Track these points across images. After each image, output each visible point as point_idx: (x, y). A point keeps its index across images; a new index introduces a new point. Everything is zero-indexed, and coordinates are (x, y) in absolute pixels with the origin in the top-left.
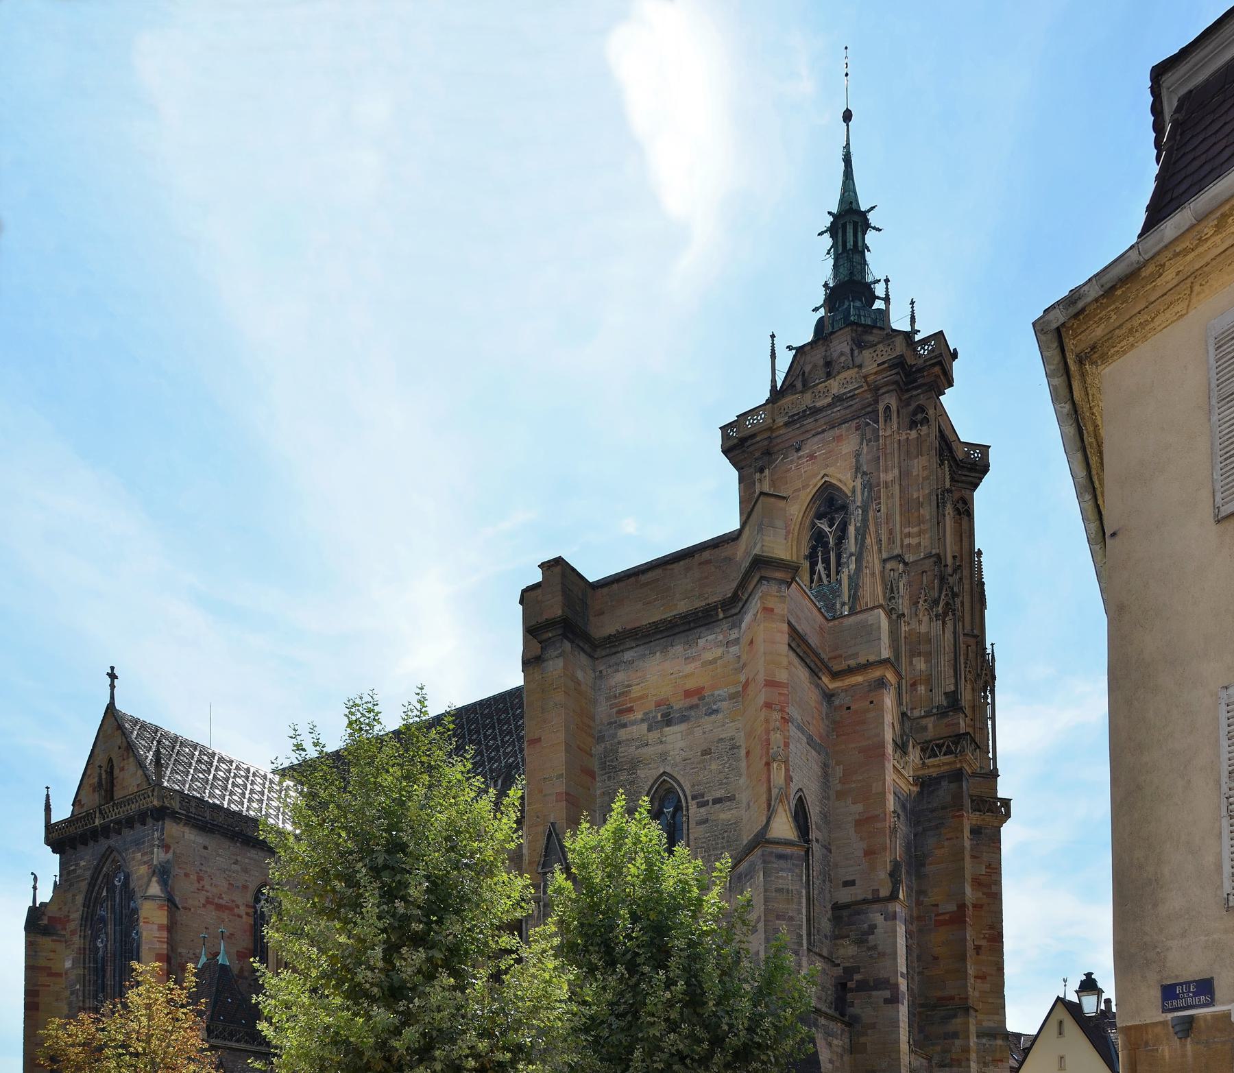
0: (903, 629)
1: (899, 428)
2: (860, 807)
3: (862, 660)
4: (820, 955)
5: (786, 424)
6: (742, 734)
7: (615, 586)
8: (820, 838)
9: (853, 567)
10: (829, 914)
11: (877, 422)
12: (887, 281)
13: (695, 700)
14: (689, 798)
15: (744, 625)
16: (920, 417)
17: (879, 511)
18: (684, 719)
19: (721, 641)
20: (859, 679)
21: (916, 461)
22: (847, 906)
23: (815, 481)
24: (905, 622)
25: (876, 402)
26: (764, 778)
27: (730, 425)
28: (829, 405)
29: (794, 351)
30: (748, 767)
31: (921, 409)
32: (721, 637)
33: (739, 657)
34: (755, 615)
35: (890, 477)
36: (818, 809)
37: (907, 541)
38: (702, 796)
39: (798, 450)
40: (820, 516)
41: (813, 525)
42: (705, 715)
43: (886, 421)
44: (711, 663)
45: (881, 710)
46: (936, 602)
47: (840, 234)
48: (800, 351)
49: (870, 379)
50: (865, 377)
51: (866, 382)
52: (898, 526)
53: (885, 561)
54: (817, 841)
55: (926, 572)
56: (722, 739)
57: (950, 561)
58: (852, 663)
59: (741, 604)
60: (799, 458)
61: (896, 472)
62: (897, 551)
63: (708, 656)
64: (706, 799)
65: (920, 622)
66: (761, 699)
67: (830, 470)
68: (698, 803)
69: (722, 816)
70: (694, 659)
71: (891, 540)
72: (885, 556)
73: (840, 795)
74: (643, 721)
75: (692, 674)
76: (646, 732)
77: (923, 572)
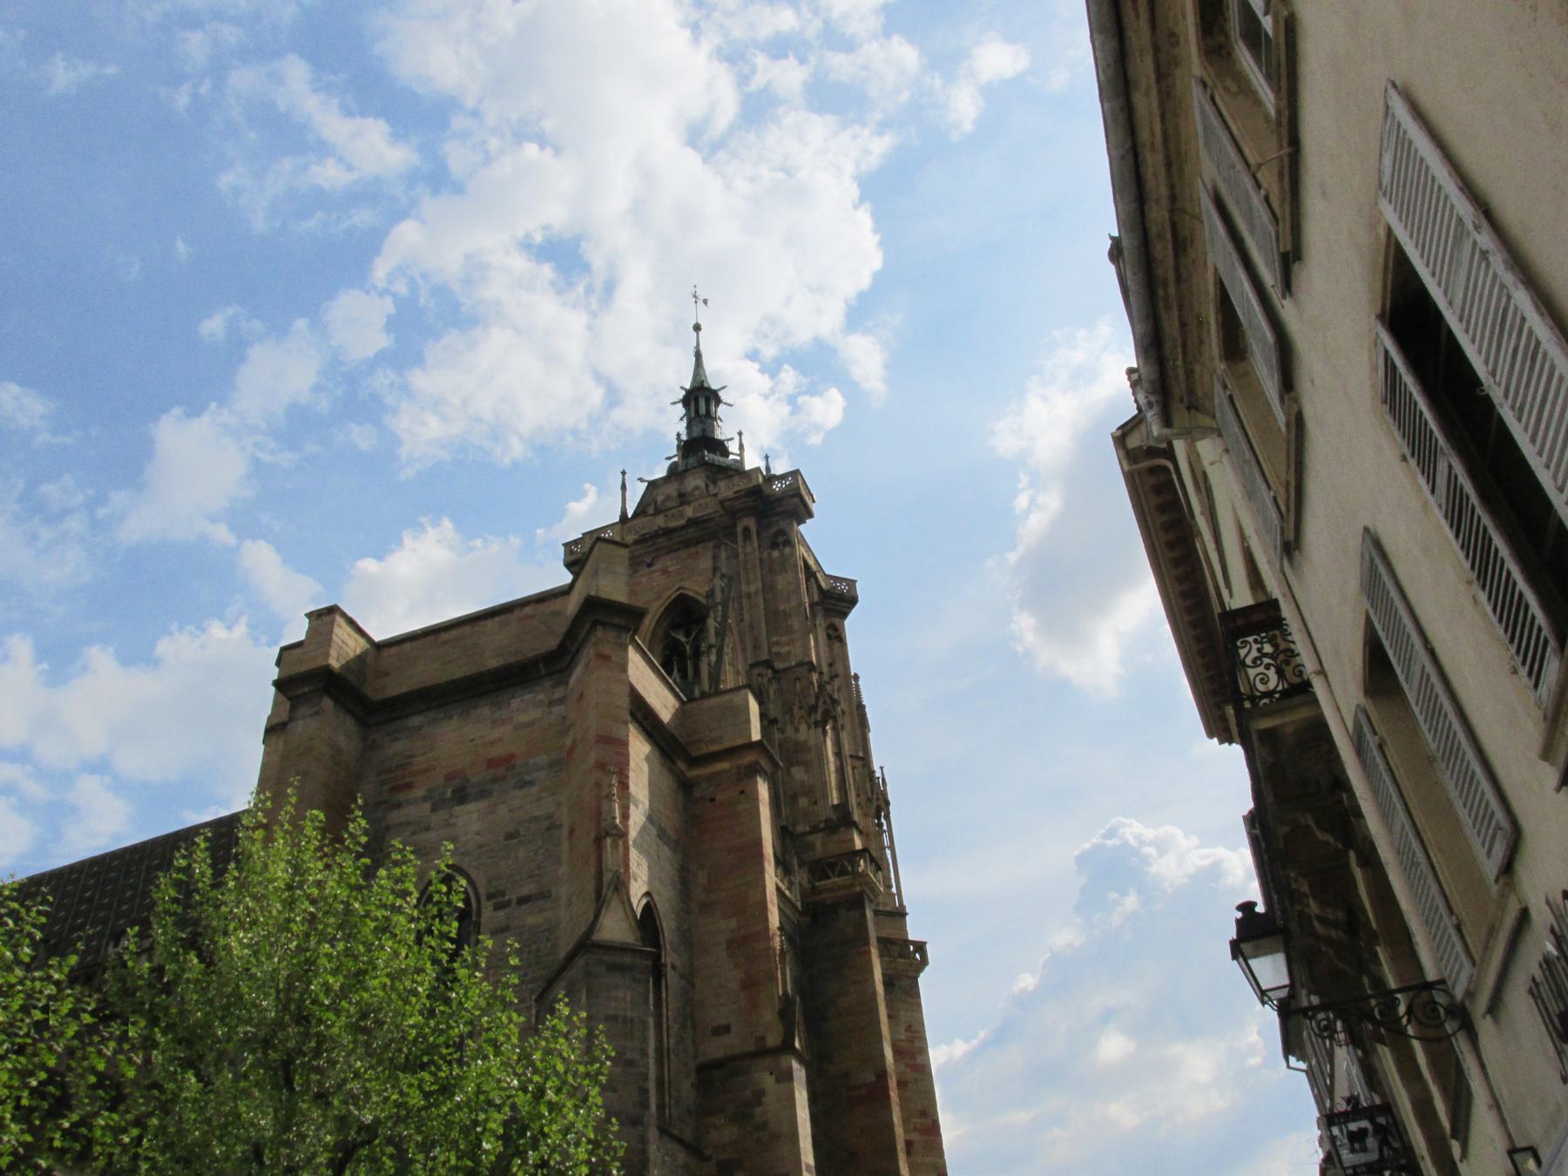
0: (776, 735)
1: (759, 547)
2: (733, 923)
3: (727, 744)
4: (680, 1141)
5: (637, 542)
6: (565, 810)
7: (407, 646)
8: (678, 964)
9: (713, 658)
10: (693, 1077)
11: (736, 543)
12: (740, 434)
13: (501, 771)
14: (483, 898)
15: (572, 681)
16: (781, 539)
17: (742, 621)
18: (483, 794)
19: (540, 701)
20: (723, 766)
21: (780, 578)
22: (718, 1065)
23: (669, 593)
24: (778, 729)
25: (735, 526)
26: (593, 861)
27: (575, 542)
28: (683, 527)
29: (646, 484)
30: (571, 849)
31: (783, 533)
32: (541, 697)
33: (564, 718)
34: (587, 666)
35: (753, 589)
36: (673, 924)
37: (775, 649)
38: (502, 894)
39: (650, 565)
40: (675, 627)
41: (667, 635)
42: (515, 788)
43: (745, 540)
44: (527, 725)
45: (755, 799)
46: (813, 709)
47: (693, 404)
48: (652, 485)
49: (727, 504)
50: (722, 502)
51: (723, 507)
52: (764, 635)
53: (753, 666)
54: (674, 967)
55: (799, 679)
56: (535, 818)
57: (825, 669)
58: (715, 748)
59: (569, 658)
60: (651, 572)
61: (759, 584)
62: (765, 657)
63: (523, 718)
64: (507, 898)
65: (797, 730)
66: (592, 758)
67: (686, 584)
68: (495, 904)
69: (531, 920)
70: (503, 722)
71: (756, 647)
72: (750, 662)
73: (706, 908)
74: (425, 799)
75: (500, 740)
76: (428, 813)
77: (796, 680)
